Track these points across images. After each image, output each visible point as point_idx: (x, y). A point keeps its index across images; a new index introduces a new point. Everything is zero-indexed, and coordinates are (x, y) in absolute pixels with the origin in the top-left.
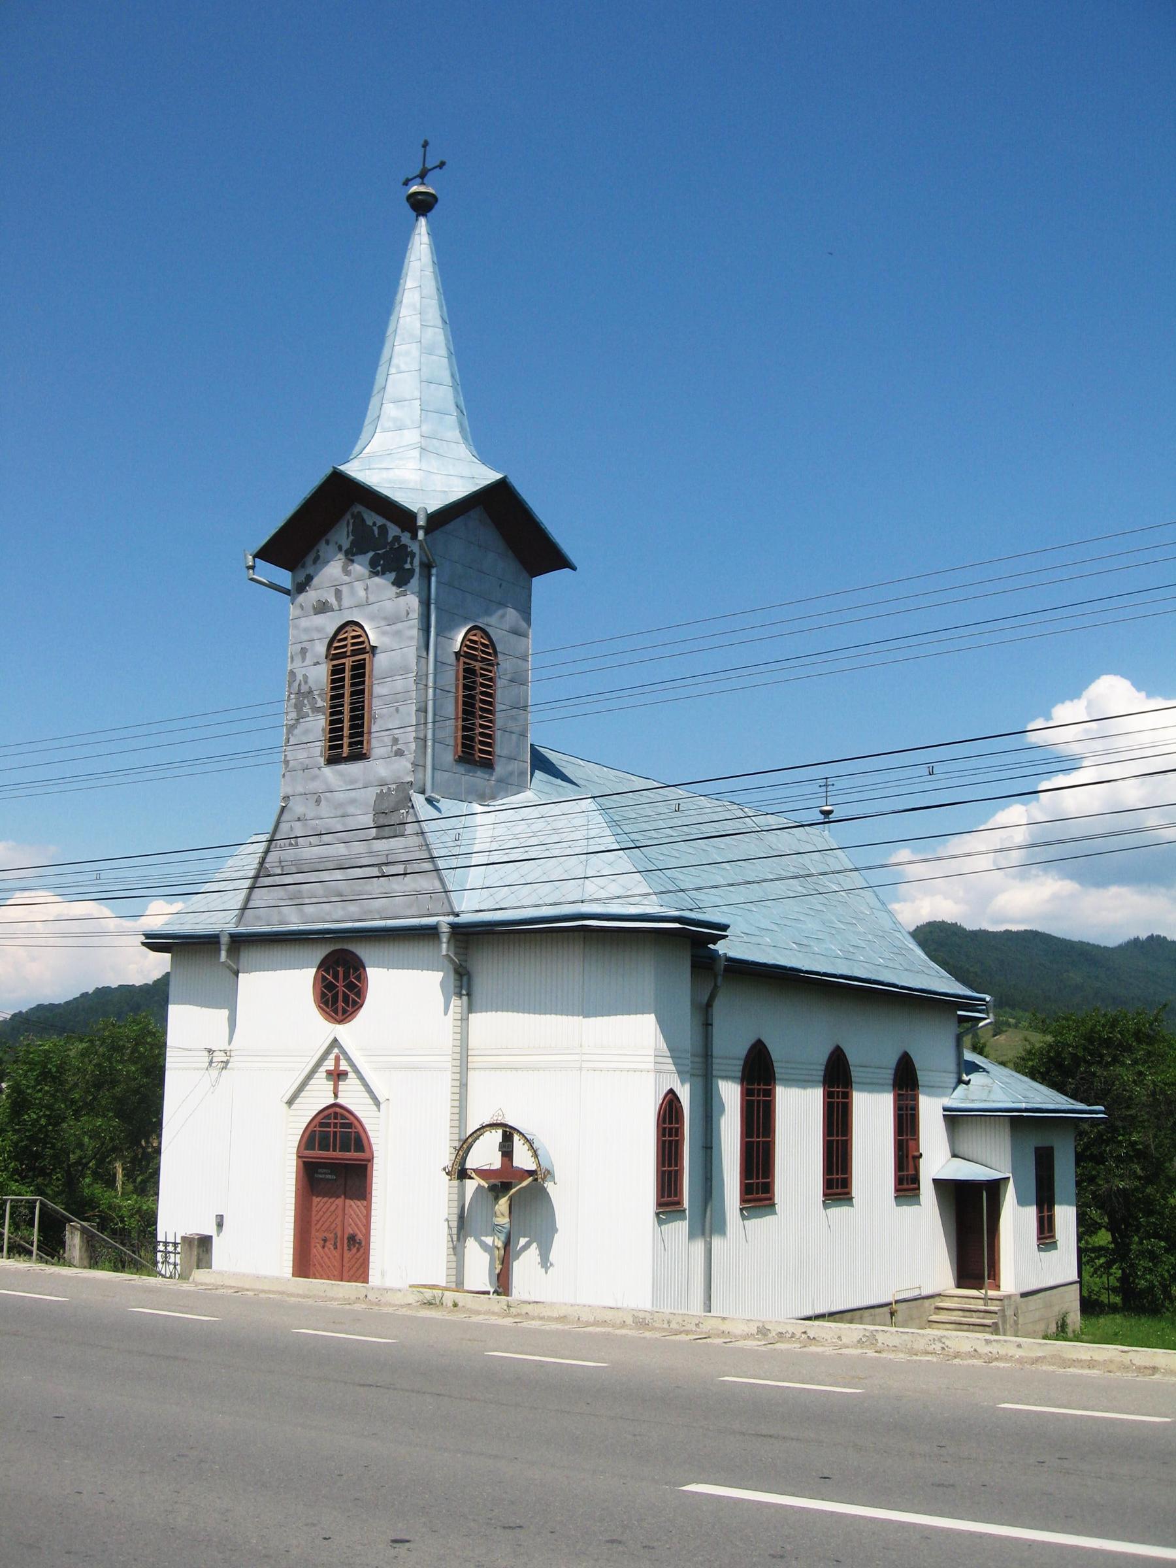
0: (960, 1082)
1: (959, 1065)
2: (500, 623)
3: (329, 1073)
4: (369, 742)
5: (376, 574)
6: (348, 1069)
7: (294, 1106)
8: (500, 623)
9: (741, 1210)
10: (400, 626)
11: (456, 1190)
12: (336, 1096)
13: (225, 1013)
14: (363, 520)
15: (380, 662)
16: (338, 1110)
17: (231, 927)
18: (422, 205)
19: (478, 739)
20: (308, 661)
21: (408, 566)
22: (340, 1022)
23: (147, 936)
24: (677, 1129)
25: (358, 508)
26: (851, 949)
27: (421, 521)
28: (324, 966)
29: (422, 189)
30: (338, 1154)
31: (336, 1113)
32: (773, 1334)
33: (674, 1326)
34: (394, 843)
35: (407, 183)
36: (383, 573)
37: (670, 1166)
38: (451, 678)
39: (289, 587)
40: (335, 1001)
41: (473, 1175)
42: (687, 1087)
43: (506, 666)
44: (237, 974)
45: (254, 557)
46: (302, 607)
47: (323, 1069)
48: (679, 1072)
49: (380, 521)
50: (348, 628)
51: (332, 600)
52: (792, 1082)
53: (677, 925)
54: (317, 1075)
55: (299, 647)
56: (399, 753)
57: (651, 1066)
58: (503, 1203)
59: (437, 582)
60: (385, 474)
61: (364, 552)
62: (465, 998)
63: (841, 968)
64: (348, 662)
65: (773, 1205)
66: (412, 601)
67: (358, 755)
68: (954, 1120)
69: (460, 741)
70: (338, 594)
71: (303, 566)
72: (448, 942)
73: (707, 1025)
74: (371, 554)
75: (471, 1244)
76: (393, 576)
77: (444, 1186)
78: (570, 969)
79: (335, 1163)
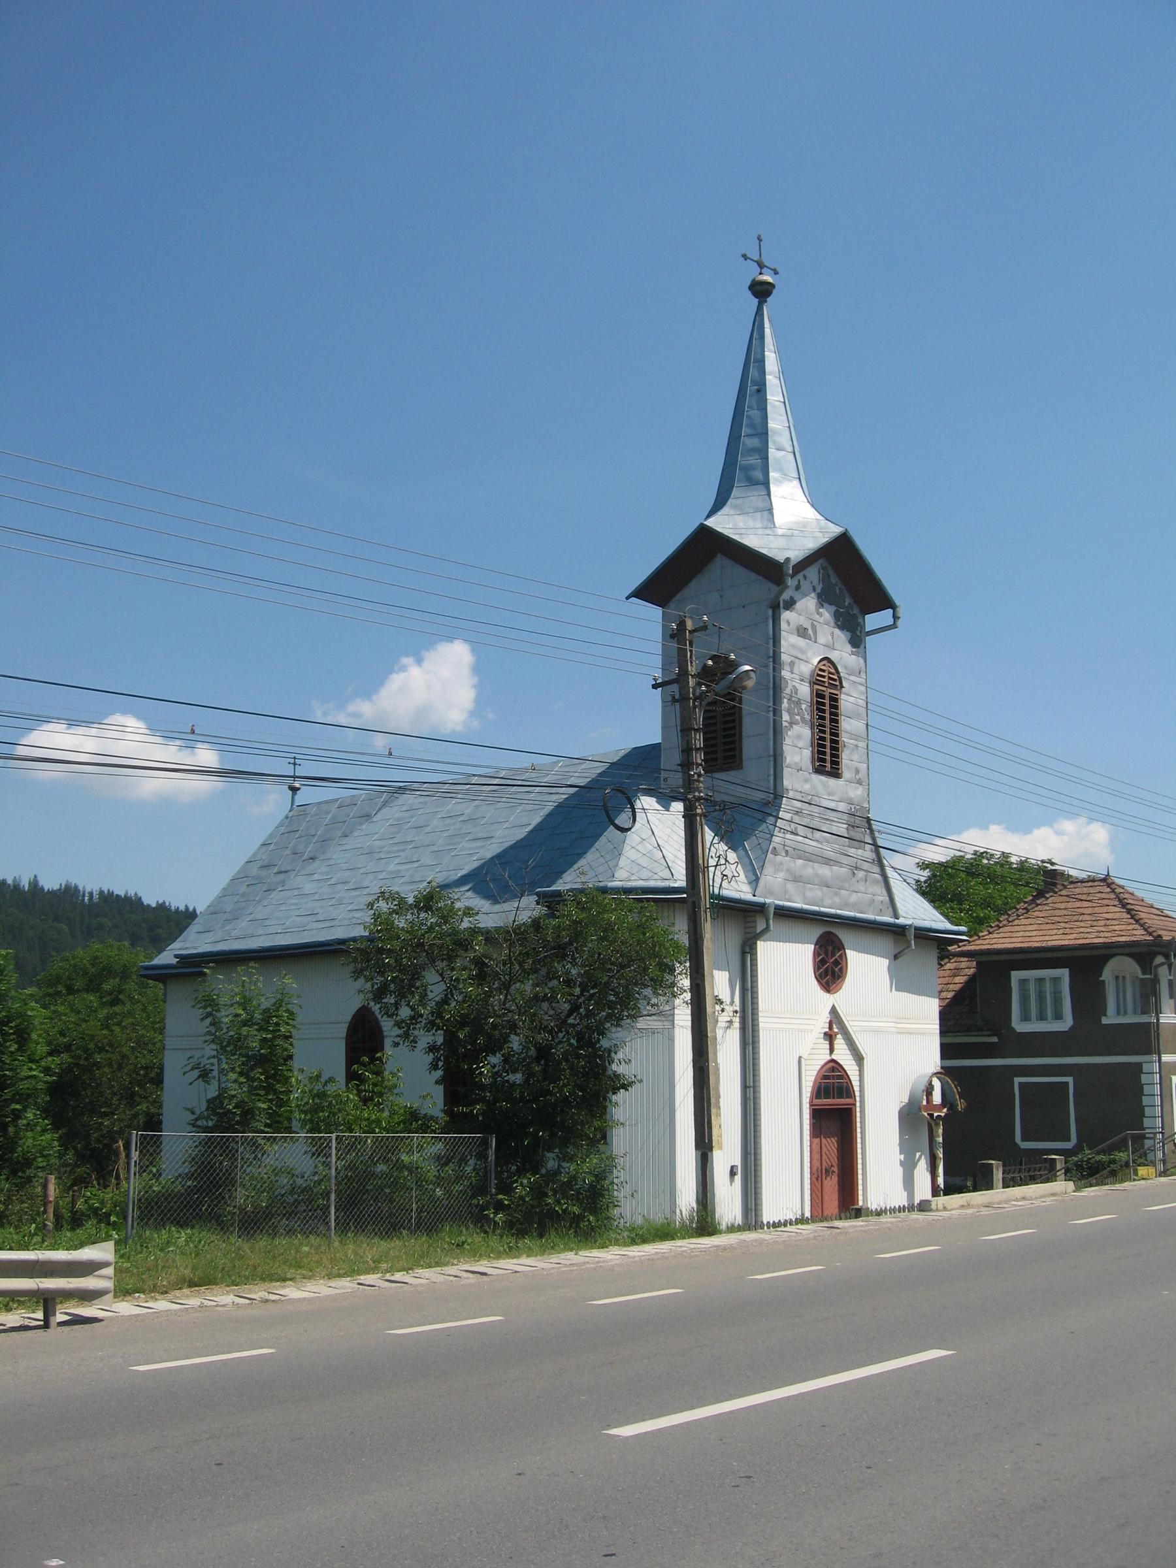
12: (832, 1050)
46: (788, 622)
49: (840, 585)
56: (859, 782)
67: (835, 773)
76: (849, 634)
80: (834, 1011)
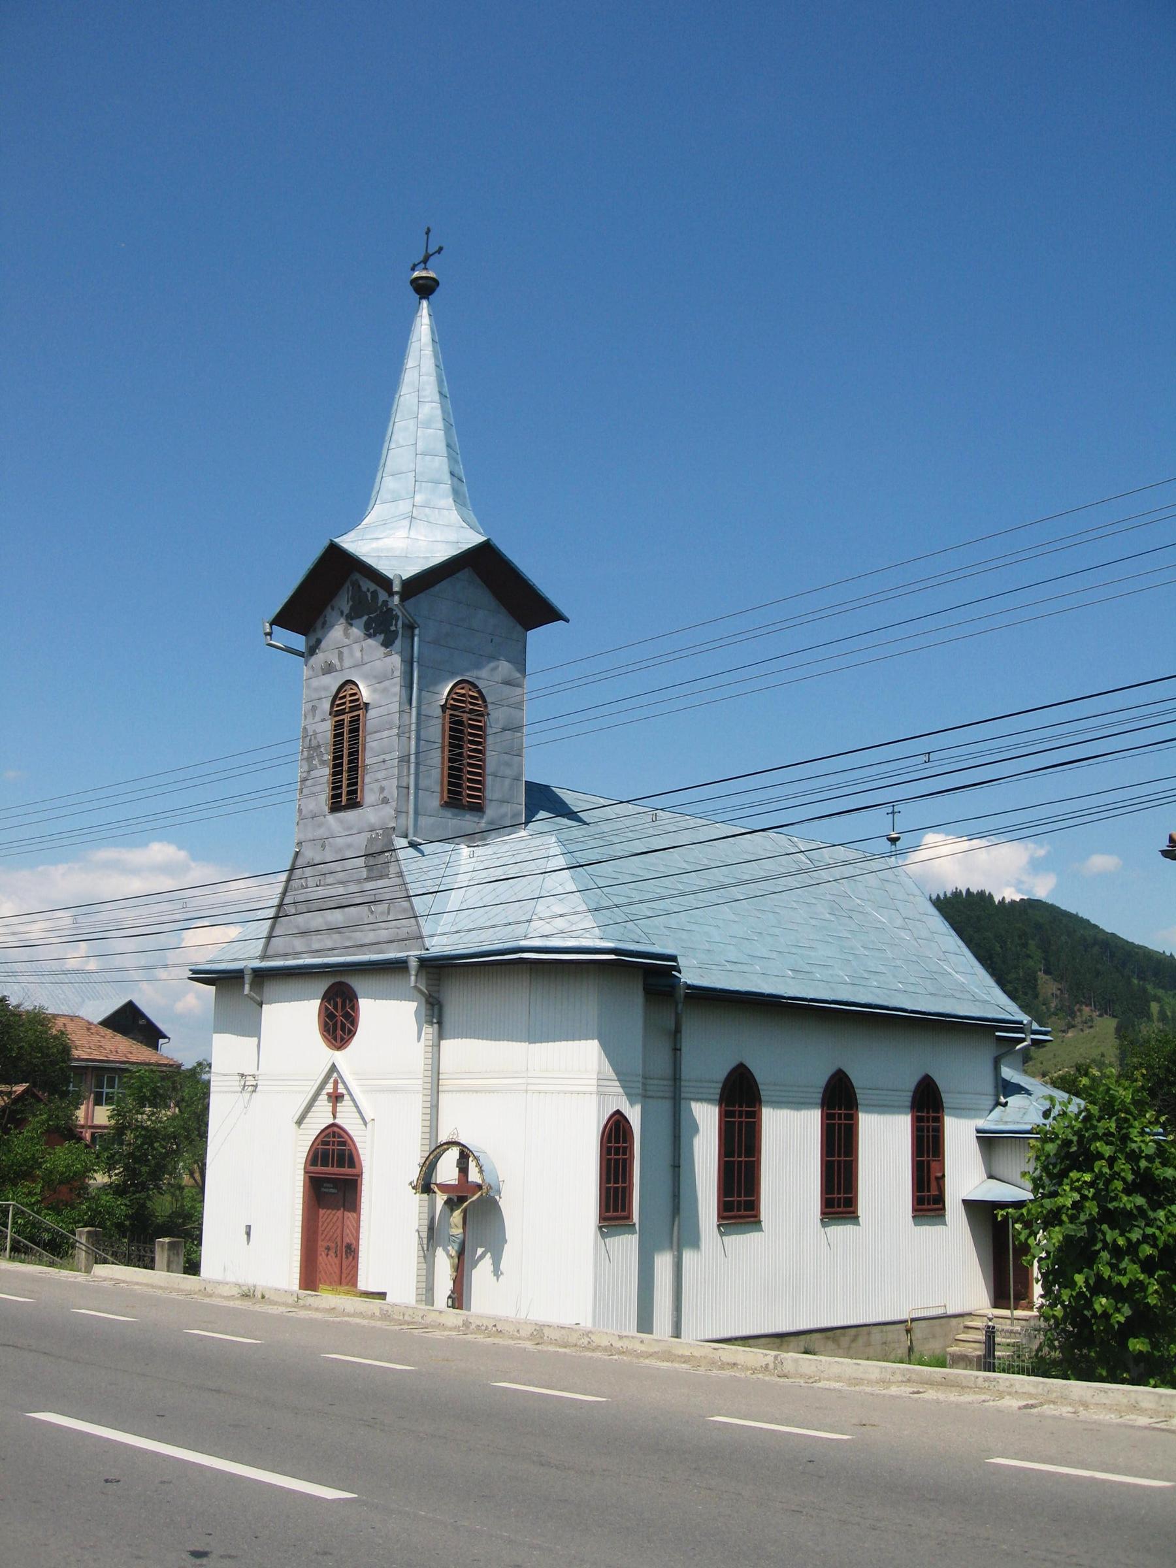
0: (998, 1104)
1: (996, 1087)
2: (491, 677)
3: (329, 1095)
4: (362, 791)
5: (369, 636)
6: (344, 1091)
7: (303, 1126)
8: (491, 677)
9: (719, 1226)
10: (387, 683)
11: (426, 1204)
12: (335, 1117)
13: (256, 1039)
14: (359, 587)
15: (372, 718)
16: (336, 1129)
17: (257, 964)
18: (425, 289)
19: (465, 782)
20: (317, 719)
21: (393, 628)
22: (339, 1048)
23: (194, 972)
24: (625, 1148)
25: (356, 576)
26: (866, 975)
27: (396, 587)
28: (327, 997)
29: (424, 274)
30: (336, 1170)
31: (334, 1132)
32: (473, 1326)
33: (406, 1318)
34: (380, 883)
35: (413, 269)
36: (375, 635)
37: (616, 1182)
38: (436, 731)
39: (303, 649)
40: (335, 1030)
41: (436, 1189)
42: (638, 1108)
43: (497, 717)
44: (261, 1005)
45: (271, 625)
47: (324, 1092)
48: (628, 1095)
50: (347, 687)
51: (335, 661)
52: (778, 1104)
53: (613, 957)
54: (320, 1097)
55: (311, 704)
56: (385, 801)
57: (594, 1089)
58: (457, 1215)
59: (420, 641)
60: (375, 545)
61: (360, 617)
62: (436, 1026)
63: (844, 994)
64: (346, 718)
65: (760, 1222)
66: (396, 660)
67: (354, 803)
68: (989, 1142)
69: (446, 788)
70: (340, 655)
71: (315, 630)
72: (417, 975)
73: (676, 1050)
74: (365, 618)
75: (440, 1253)
76: (381, 637)
77: (416, 1201)
78: (518, 998)
79: (333, 1178)
80: (333, 1068)
